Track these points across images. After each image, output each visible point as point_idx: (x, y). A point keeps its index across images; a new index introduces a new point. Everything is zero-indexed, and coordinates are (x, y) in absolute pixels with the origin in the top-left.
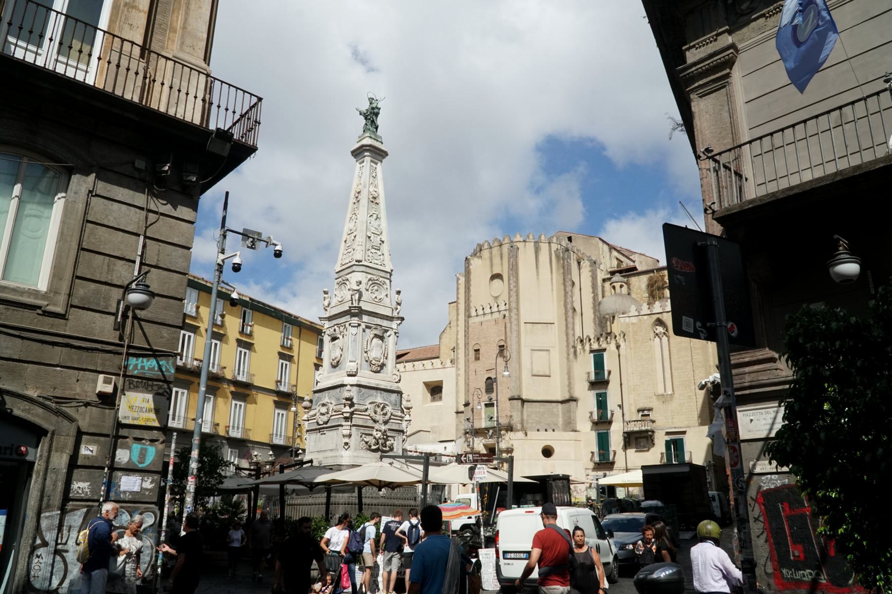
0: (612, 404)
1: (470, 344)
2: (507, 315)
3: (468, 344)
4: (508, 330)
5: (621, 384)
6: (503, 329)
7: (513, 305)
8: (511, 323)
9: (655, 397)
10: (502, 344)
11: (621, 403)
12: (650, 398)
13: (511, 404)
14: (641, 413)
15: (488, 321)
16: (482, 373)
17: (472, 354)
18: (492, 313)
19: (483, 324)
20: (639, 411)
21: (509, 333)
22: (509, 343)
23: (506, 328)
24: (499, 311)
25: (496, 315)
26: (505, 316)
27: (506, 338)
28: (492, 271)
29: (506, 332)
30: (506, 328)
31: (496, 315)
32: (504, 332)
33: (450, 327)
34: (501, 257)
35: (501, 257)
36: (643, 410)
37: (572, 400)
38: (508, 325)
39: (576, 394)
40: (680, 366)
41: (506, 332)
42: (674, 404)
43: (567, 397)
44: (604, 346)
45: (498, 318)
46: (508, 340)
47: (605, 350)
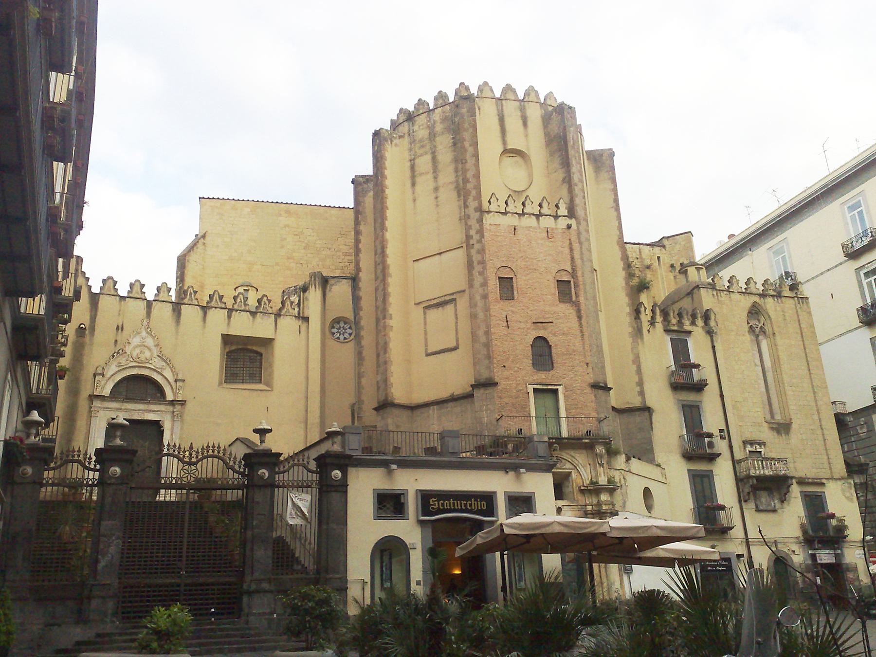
0: (711, 422)
1: (489, 264)
2: (574, 226)
3: (482, 262)
4: (577, 255)
5: (722, 396)
6: (567, 251)
7: (580, 212)
8: (580, 243)
9: (765, 425)
10: (565, 278)
11: (724, 427)
12: (760, 425)
13: (595, 396)
14: (749, 448)
15: (529, 228)
16: (523, 325)
17: (493, 284)
18: (538, 216)
19: (518, 232)
20: (745, 443)
21: (578, 262)
22: (580, 279)
23: (571, 250)
24: (556, 217)
25: (563, 222)
26: (569, 227)
27: (574, 269)
28: (504, 143)
29: (572, 258)
30: (571, 250)
31: (547, 222)
32: (569, 257)
33: (204, 244)
34: (525, 124)
35: (525, 124)
36: (752, 443)
37: (647, 410)
38: (576, 246)
39: (649, 403)
40: (794, 381)
41: (572, 258)
42: (795, 437)
43: (637, 402)
44: (687, 326)
45: (552, 229)
46: (579, 274)
47: (690, 332)
